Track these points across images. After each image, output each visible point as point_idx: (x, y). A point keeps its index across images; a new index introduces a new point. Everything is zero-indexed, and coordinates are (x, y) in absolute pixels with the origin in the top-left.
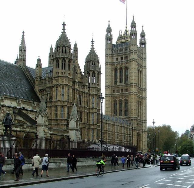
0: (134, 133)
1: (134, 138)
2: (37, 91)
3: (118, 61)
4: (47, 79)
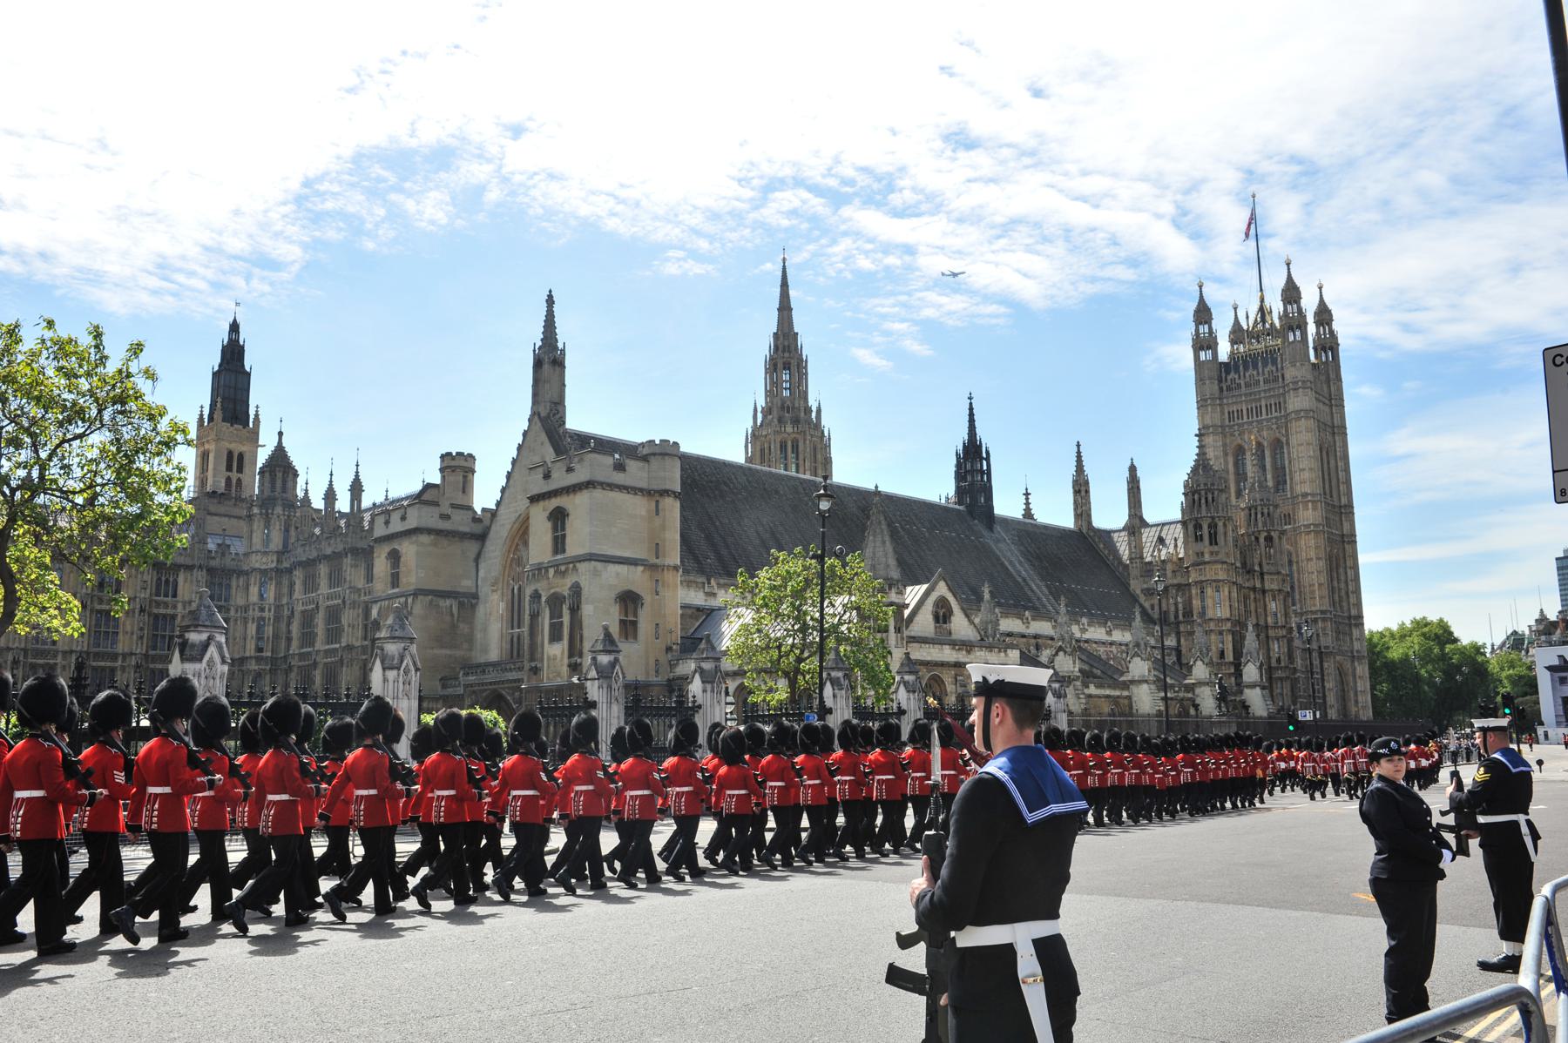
0: (1326, 665)
1: (1327, 685)
3: (1245, 419)
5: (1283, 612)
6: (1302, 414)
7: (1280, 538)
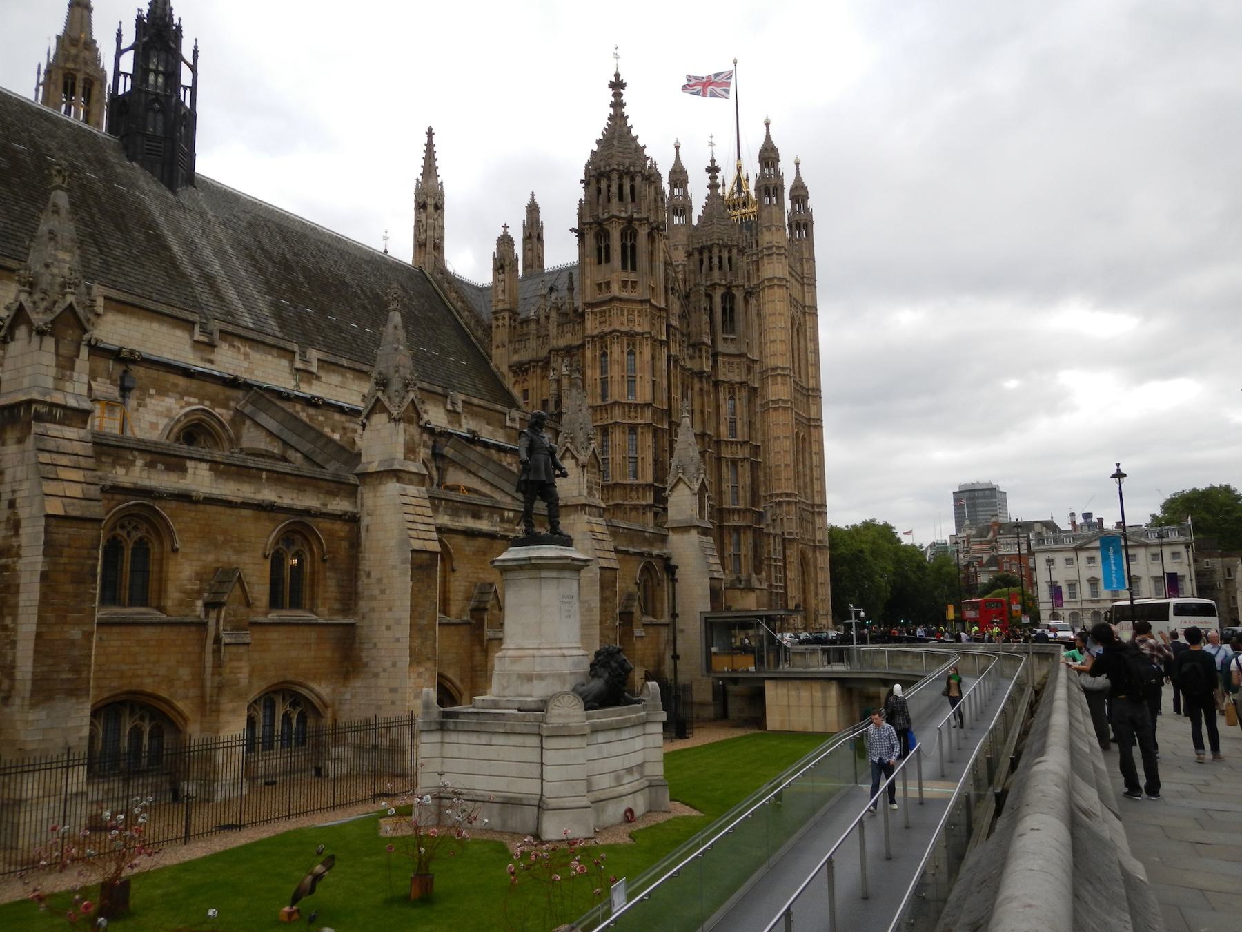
0: (788, 552)
2: (504, 369)
4: (553, 314)
5: (745, 419)
6: (776, 281)
7: (746, 302)
